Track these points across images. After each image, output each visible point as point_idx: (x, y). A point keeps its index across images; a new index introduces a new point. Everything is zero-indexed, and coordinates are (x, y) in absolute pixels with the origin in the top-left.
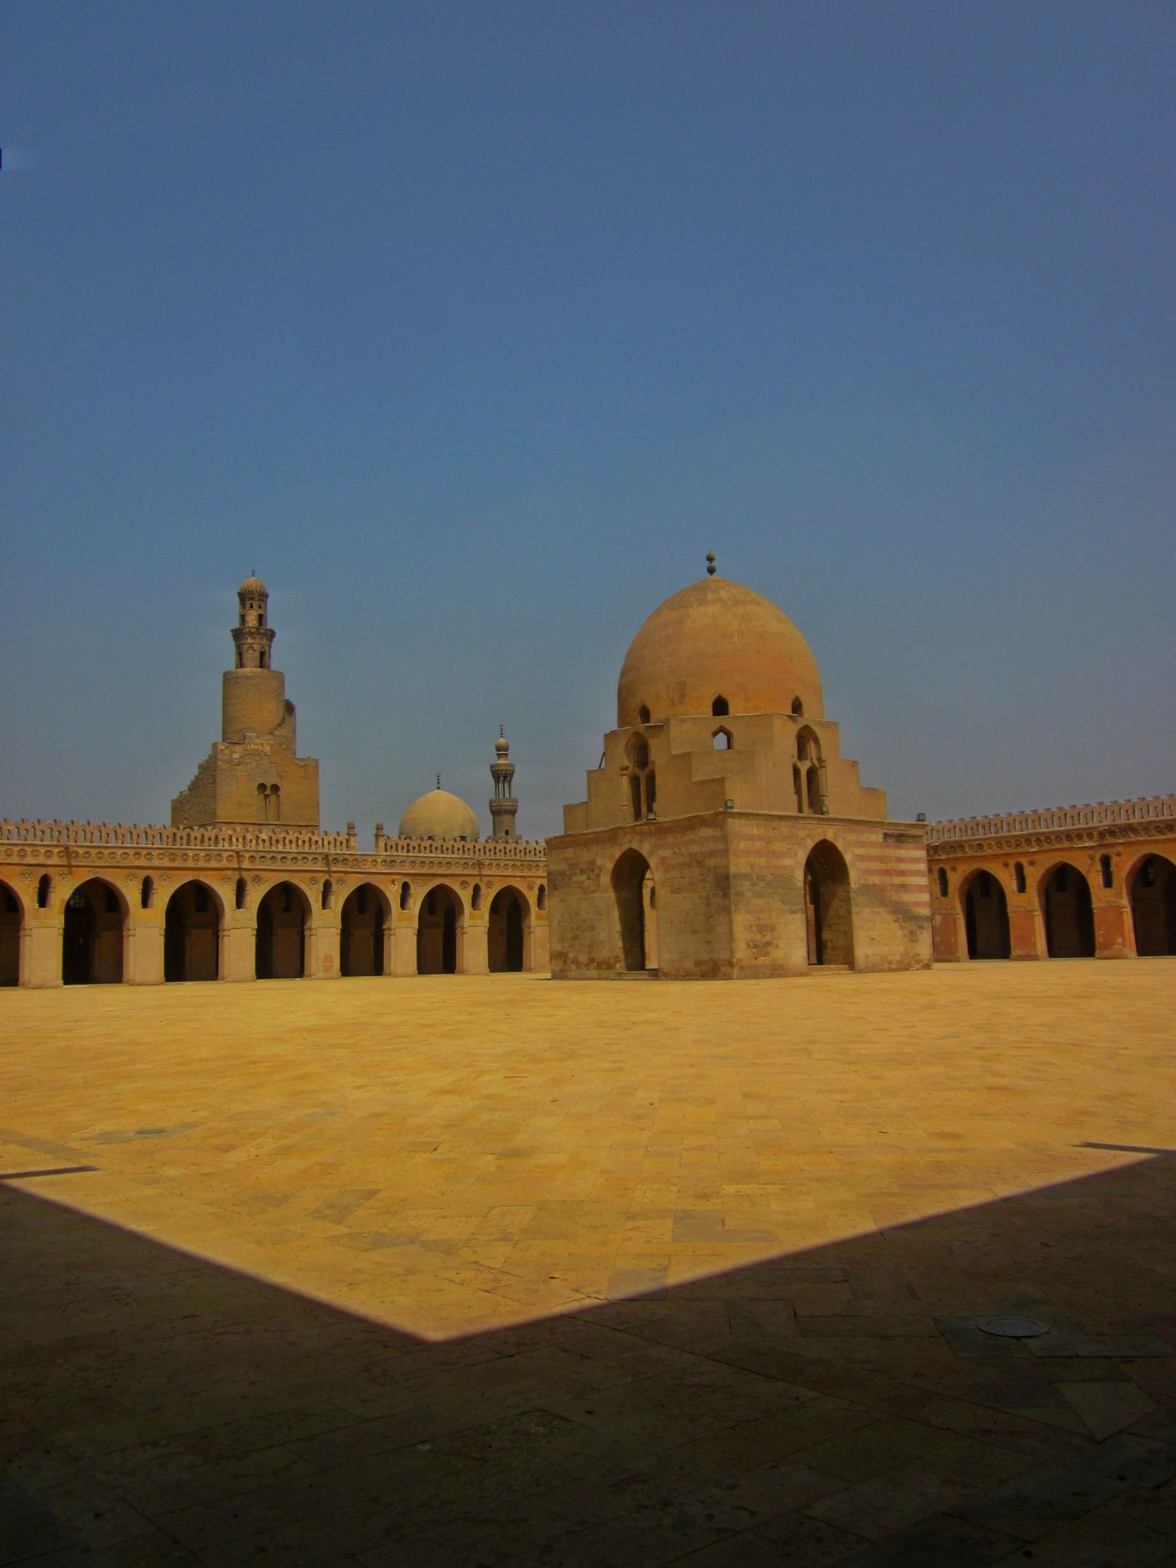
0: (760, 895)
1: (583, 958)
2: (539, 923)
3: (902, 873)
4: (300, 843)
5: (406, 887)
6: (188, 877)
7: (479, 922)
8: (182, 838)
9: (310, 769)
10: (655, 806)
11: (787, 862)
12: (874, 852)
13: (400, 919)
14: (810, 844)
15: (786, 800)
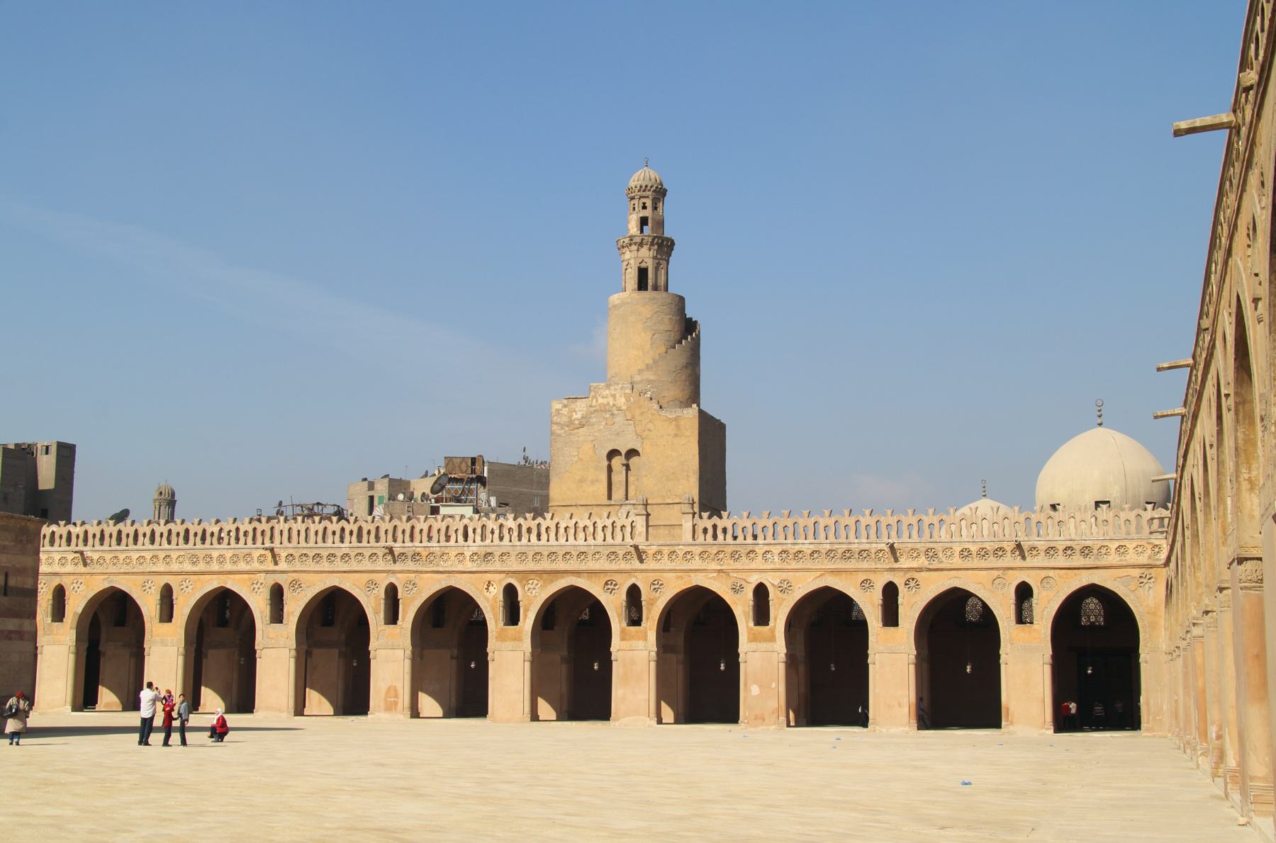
2: (754, 645)
4: (562, 531)
6: (212, 584)
7: (641, 644)
8: (334, 533)
13: (501, 637)
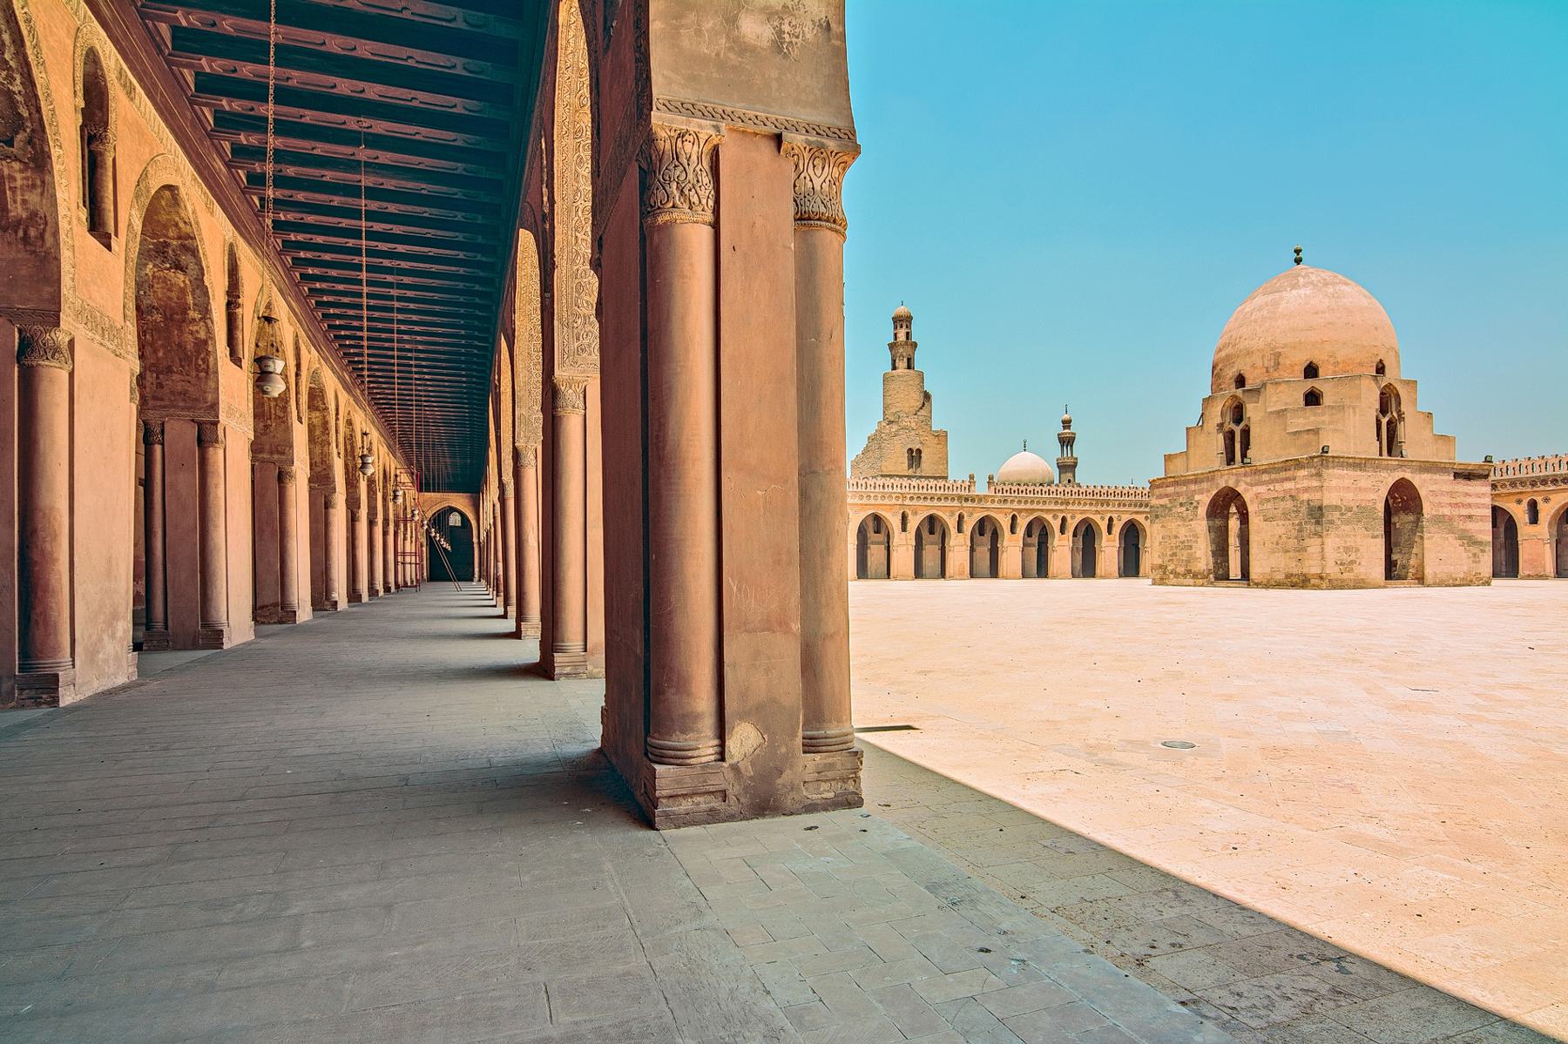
0: (1348, 522)
1: (1181, 570)
3: (1470, 505)
5: (1014, 518)
9: (942, 437)
10: (1250, 453)
11: (1373, 496)
12: (1446, 488)
14: (1391, 482)
15: (1369, 446)
